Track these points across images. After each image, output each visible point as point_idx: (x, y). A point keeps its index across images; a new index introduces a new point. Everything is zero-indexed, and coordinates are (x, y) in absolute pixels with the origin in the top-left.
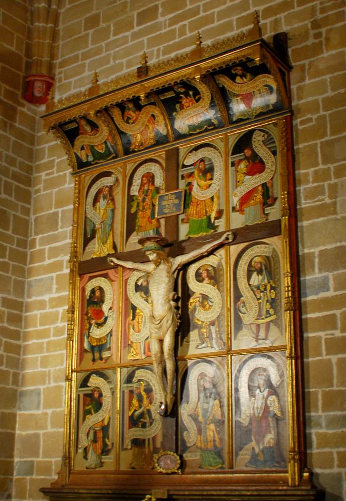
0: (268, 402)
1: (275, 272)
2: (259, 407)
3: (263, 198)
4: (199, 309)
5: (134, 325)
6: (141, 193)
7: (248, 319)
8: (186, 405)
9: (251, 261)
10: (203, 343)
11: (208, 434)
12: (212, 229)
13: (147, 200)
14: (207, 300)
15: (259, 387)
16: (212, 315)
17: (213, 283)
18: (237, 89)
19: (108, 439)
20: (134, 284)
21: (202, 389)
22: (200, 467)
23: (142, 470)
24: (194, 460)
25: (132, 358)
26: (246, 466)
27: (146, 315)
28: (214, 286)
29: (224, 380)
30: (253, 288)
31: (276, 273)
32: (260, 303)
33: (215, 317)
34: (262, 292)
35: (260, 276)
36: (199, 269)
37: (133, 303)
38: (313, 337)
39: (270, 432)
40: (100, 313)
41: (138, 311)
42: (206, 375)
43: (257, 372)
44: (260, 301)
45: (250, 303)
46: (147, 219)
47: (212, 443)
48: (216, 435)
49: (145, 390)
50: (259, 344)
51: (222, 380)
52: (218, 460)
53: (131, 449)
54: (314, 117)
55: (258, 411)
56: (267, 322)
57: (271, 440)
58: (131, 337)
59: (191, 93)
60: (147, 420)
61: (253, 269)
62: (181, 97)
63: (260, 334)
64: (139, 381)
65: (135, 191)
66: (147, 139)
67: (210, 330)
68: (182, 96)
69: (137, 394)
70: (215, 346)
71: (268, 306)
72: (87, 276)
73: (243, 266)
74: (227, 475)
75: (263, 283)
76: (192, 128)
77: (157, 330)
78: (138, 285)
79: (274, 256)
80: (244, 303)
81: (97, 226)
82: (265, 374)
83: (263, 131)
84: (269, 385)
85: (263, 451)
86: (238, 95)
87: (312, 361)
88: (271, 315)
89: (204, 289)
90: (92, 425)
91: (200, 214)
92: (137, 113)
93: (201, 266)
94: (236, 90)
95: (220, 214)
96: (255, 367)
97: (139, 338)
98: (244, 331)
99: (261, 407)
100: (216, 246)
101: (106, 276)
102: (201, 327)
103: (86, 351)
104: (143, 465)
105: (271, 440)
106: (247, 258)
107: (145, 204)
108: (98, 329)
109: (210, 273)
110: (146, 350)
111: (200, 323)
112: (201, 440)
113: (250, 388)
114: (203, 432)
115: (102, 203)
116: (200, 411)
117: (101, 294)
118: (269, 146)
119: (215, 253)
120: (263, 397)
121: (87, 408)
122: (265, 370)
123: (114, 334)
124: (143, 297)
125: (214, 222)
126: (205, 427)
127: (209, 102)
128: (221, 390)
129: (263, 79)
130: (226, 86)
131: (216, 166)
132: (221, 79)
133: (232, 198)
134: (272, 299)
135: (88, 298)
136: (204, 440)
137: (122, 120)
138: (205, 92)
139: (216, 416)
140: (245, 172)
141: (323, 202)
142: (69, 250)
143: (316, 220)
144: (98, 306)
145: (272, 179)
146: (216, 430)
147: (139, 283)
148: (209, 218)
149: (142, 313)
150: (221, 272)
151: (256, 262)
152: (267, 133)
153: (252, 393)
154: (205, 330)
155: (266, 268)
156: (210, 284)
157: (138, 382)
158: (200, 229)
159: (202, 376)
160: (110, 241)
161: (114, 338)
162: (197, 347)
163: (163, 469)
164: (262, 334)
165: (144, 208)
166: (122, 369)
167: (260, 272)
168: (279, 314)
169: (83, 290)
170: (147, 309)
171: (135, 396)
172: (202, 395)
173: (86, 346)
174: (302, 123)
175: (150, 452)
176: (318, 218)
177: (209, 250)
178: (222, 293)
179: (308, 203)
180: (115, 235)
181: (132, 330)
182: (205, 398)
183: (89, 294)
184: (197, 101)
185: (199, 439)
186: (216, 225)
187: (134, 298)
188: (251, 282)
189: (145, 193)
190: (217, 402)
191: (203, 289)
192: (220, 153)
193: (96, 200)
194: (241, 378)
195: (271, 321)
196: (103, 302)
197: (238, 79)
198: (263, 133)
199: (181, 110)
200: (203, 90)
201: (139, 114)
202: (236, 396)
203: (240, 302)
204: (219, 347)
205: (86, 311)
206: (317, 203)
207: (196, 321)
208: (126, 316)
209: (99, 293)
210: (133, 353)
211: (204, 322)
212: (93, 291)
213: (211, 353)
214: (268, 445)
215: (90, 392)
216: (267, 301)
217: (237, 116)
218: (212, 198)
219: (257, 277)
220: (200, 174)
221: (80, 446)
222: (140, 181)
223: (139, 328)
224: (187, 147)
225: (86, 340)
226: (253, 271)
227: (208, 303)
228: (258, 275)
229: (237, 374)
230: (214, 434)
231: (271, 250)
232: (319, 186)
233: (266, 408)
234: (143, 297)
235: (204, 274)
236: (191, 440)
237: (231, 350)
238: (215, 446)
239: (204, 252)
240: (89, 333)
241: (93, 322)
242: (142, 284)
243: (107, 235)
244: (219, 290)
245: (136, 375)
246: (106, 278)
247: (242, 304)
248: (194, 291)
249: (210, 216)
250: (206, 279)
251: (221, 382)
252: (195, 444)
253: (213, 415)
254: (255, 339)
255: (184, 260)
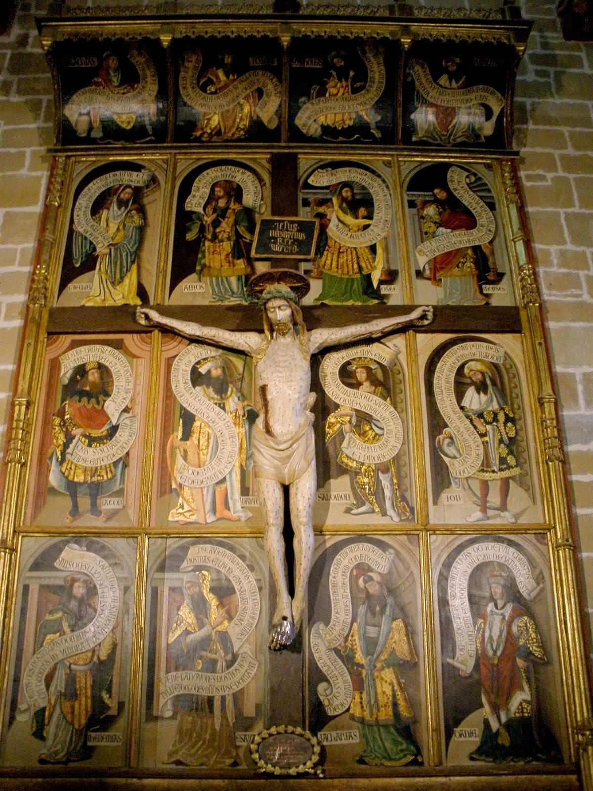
0: (515, 629)
1: (511, 392)
2: (495, 637)
3: (477, 268)
4: (350, 438)
5: (185, 451)
6: (210, 210)
7: (462, 468)
8: (322, 626)
9: (461, 368)
10: (363, 504)
11: (379, 690)
12: (374, 298)
13: (224, 224)
14: (369, 422)
15: (492, 599)
16: (382, 452)
17: (381, 394)
18: (433, 93)
19: (109, 691)
20: (189, 369)
21: (364, 596)
22: (361, 761)
23: (204, 767)
24: (344, 745)
25: (181, 518)
26: (472, 759)
27: (218, 434)
28: (385, 399)
29: (414, 581)
30: (470, 414)
31: (514, 395)
32: (485, 444)
33: (388, 457)
34: (487, 423)
35: (482, 394)
36: (348, 363)
37: (185, 406)
38: (585, 515)
39: (522, 689)
40: (98, 416)
41: (197, 424)
42: (370, 569)
43: (489, 569)
44: (486, 439)
45: (465, 441)
46: (223, 257)
47: (390, 709)
48: (399, 693)
49: (213, 590)
50: (488, 518)
51: (410, 579)
52: (404, 746)
53: (173, 717)
54: (550, 175)
55: (492, 647)
56: (502, 479)
57: (525, 706)
58: (177, 475)
59: (352, 74)
60: (220, 655)
61: (469, 381)
62: (331, 75)
63: (489, 499)
64: (198, 568)
65: (195, 202)
66: (232, 127)
67: (379, 482)
68: (334, 73)
69: (192, 598)
70: (390, 512)
71: (504, 451)
72: (67, 339)
73: (446, 372)
74: (433, 779)
75: (490, 408)
76: (329, 132)
77: (279, 463)
78: (200, 373)
79: (508, 366)
80: (451, 438)
81: (98, 250)
82: (504, 574)
83: (468, 170)
84: (513, 594)
85: (509, 726)
86: (432, 105)
87: (588, 557)
88: (509, 467)
89: (364, 402)
90: (61, 657)
91: (346, 269)
92: (231, 77)
93: (354, 359)
94: (431, 94)
95: (391, 277)
96: (481, 560)
97: (200, 477)
98: (454, 490)
99: (500, 636)
100: (400, 326)
101: (118, 345)
102: (357, 474)
103: (53, 491)
104: (206, 756)
105: (525, 706)
106: (453, 359)
107: (218, 230)
108: (90, 450)
109: (375, 376)
110: (219, 505)
111: (355, 464)
112: (361, 703)
113: (473, 600)
114: (366, 685)
115: (113, 215)
116: (357, 642)
117: (101, 378)
118: (480, 194)
119: (383, 341)
120: (504, 618)
121: (48, 617)
122: (502, 566)
123: (133, 462)
124: (213, 398)
125: (378, 287)
126: (372, 675)
127: (376, 99)
128: (407, 601)
129: (483, 94)
130: (417, 83)
131: (377, 200)
132: (417, 68)
133: (415, 257)
134: (510, 439)
135: (66, 381)
136: (369, 702)
137: (195, 82)
138: (377, 80)
139: (398, 654)
140: (437, 221)
141: (580, 299)
142: (24, 284)
143: (572, 324)
144: (93, 400)
145: (491, 242)
146: (399, 684)
147: (203, 370)
148: (368, 278)
149: (207, 429)
150: (400, 376)
151: (471, 370)
152: (475, 175)
153: (478, 610)
154: (366, 480)
155: (494, 384)
156: (374, 393)
157: (194, 571)
158: (348, 293)
159: (362, 569)
160: (131, 280)
161: (133, 471)
162: (348, 511)
163: (274, 766)
164: (494, 498)
165: (215, 237)
166: (152, 540)
167: (482, 388)
168: (526, 467)
169: (55, 365)
170: (221, 423)
171: (187, 601)
172: (362, 609)
173: (54, 479)
174: (529, 178)
175: (228, 725)
176: (574, 321)
177: (386, 330)
178: (404, 415)
179: (555, 295)
180: (143, 271)
181: (180, 460)
182: (369, 615)
183: (68, 375)
184: (355, 91)
185: (357, 699)
186: (382, 292)
187: (187, 396)
188: (465, 402)
189: (219, 212)
190: (399, 623)
191: (358, 401)
192: (384, 181)
193: (98, 206)
194: (454, 579)
195: (513, 478)
196: (107, 395)
197: (444, 80)
198: (467, 174)
199: (317, 97)
200: (377, 76)
201: (234, 80)
202: (443, 614)
203: (441, 437)
204: (399, 515)
205: (58, 405)
206: (569, 299)
207: (345, 460)
208: (167, 431)
209: (96, 375)
210: (182, 507)
211: (363, 464)
212: (81, 371)
213: (384, 525)
214: (517, 715)
215: (61, 582)
216: (501, 441)
217: (420, 135)
218: (373, 249)
219: (476, 395)
220: (344, 205)
221: (22, 706)
222: (208, 191)
223: (199, 458)
224: (314, 159)
225: (54, 467)
226: (470, 385)
227: (371, 428)
228: (479, 393)
229: (444, 571)
230: (394, 691)
231: (502, 354)
232: (569, 274)
233: (510, 639)
234: (210, 398)
235: (361, 375)
236: (336, 702)
237: (428, 523)
238: (396, 714)
239: (376, 332)
240: (63, 454)
241: (77, 432)
242: (209, 372)
243: (125, 269)
244: (395, 408)
245: (189, 555)
246: (117, 348)
247: (447, 441)
248: (337, 401)
249: (369, 276)
250: (366, 384)
251: (407, 584)
252: (348, 710)
253: (388, 651)
254: (479, 508)
255: (333, 337)
